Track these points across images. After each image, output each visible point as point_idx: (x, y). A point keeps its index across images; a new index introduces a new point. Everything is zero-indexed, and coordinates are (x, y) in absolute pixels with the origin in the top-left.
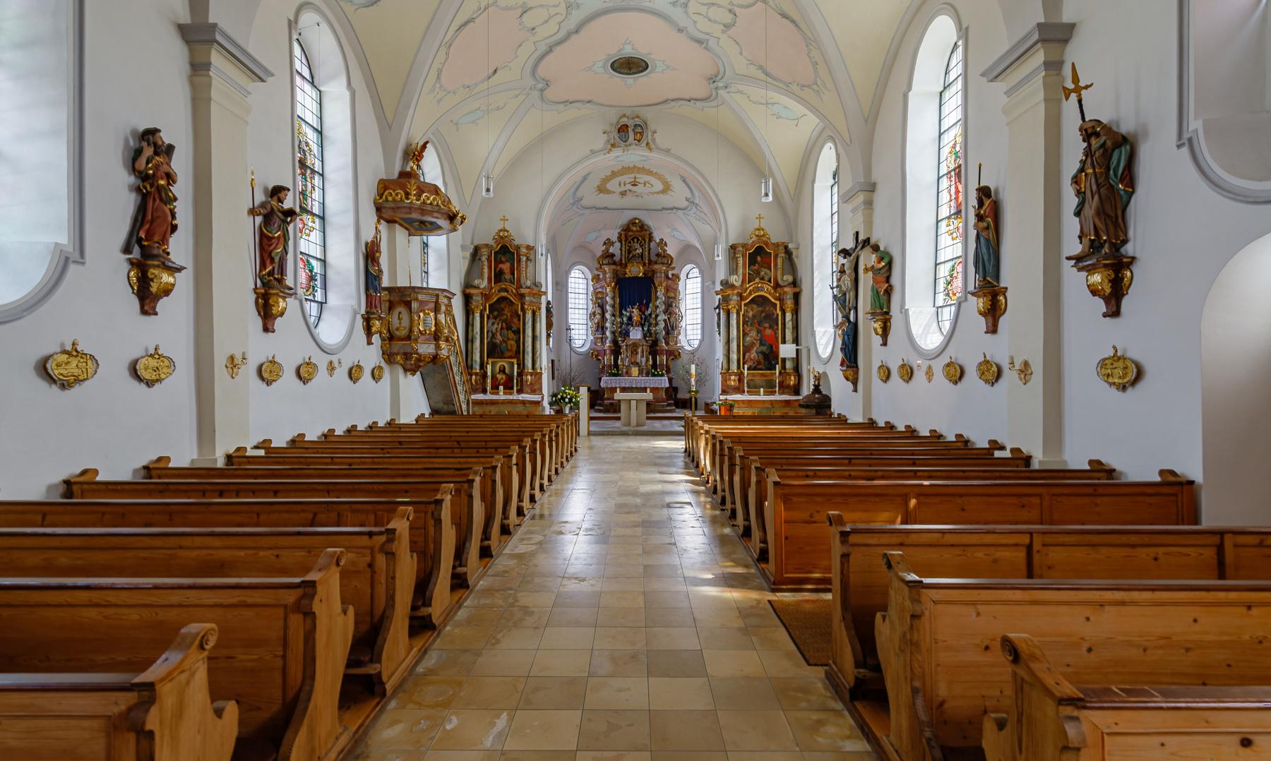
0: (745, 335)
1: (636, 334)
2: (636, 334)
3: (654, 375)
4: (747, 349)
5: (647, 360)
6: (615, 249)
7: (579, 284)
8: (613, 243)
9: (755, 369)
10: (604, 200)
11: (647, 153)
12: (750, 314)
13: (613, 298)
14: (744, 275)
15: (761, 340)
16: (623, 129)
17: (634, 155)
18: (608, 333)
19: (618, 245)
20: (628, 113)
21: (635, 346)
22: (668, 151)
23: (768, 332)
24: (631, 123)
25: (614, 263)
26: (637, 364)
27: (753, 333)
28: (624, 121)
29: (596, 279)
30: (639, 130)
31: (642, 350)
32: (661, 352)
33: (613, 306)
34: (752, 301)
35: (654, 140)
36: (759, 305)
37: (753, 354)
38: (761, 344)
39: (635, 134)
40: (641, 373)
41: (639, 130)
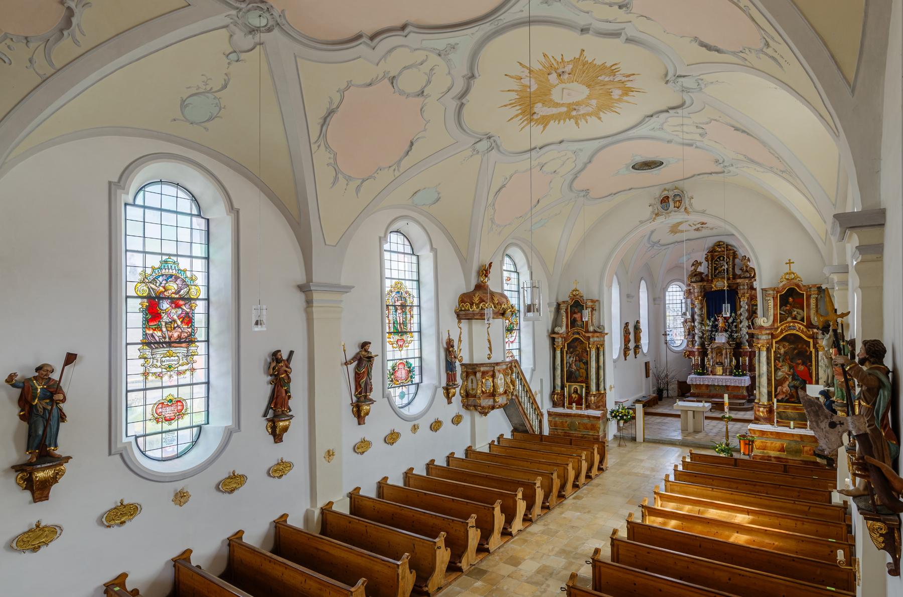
0: (776, 369)
1: (721, 339)
2: (721, 339)
3: (735, 375)
4: (779, 383)
5: (731, 361)
6: (701, 269)
7: (676, 297)
8: (700, 264)
9: (787, 401)
10: (678, 237)
11: (686, 217)
12: (782, 351)
13: (701, 309)
14: (775, 316)
15: (793, 375)
16: (665, 200)
17: (676, 217)
18: (696, 338)
19: (705, 264)
20: (667, 187)
21: (719, 351)
22: (703, 212)
23: (801, 368)
24: (671, 194)
25: (702, 280)
26: (721, 364)
27: (786, 369)
28: (666, 192)
29: (689, 293)
30: (678, 198)
31: (727, 351)
32: (745, 354)
33: (700, 315)
34: (784, 339)
35: (691, 205)
36: (790, 343)
37: (785, 388)
38: (793, 379)
39: (675, 202)
40: (724, 372)
41: (678, 198)
